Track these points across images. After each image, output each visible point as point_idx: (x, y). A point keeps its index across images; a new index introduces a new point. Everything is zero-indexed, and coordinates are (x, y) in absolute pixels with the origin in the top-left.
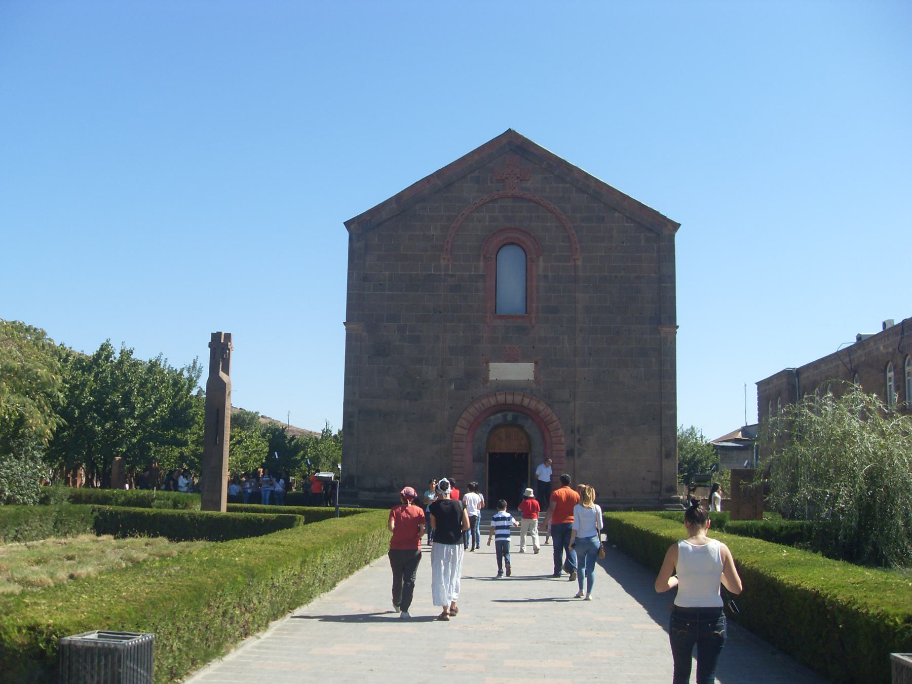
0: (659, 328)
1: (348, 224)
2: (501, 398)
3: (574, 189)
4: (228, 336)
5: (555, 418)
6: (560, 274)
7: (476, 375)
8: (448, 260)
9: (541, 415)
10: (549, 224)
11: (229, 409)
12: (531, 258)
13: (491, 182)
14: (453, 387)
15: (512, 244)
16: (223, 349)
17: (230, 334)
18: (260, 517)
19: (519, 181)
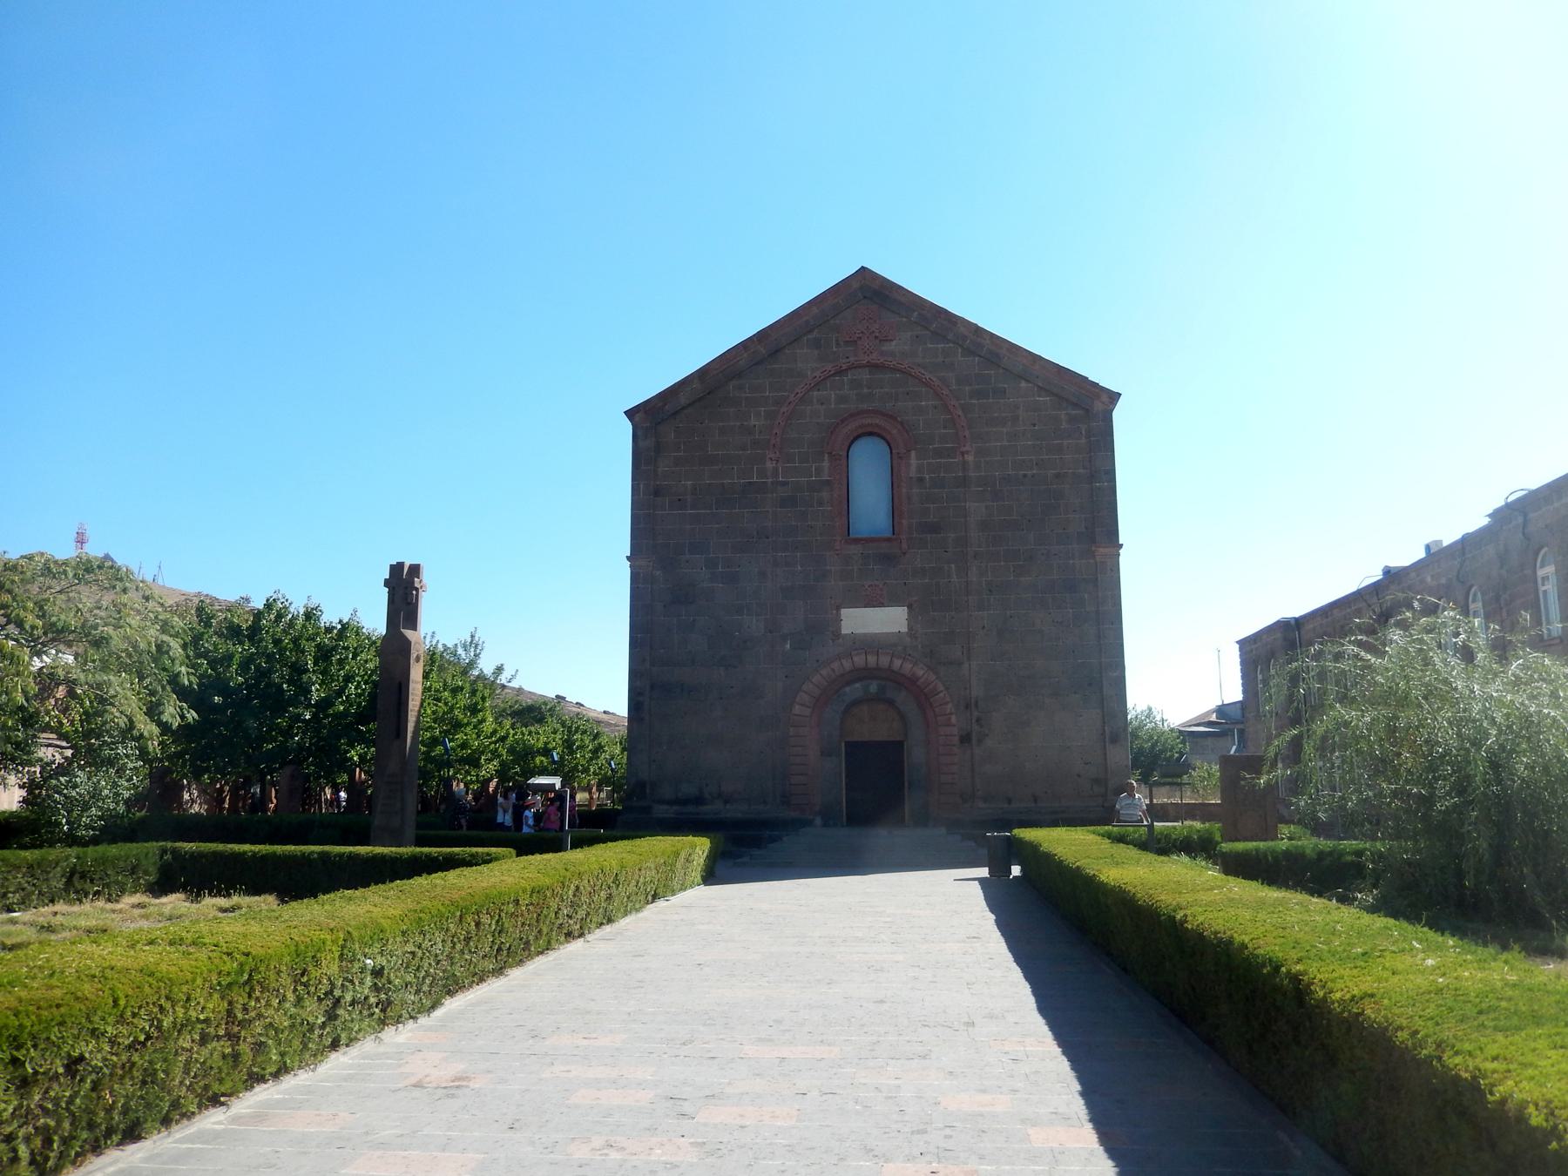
0: (1093, 548)
1: (630, 414)
2: (859, 660)
3: (960, 350)
4: (415, 570)
5: (941, 687)
6: (942, 475)
7: (823, 627)
8: (777, 461)
9: (918, 683)
10: (923, 403)
11: (417, 682)
12: (898, 453)
13: (838, 345)
14: (788, 646)
15: (870, 434)
16: (406, 588)
17: (419, 565)
18: (436, 855)
19: (877, 341)
